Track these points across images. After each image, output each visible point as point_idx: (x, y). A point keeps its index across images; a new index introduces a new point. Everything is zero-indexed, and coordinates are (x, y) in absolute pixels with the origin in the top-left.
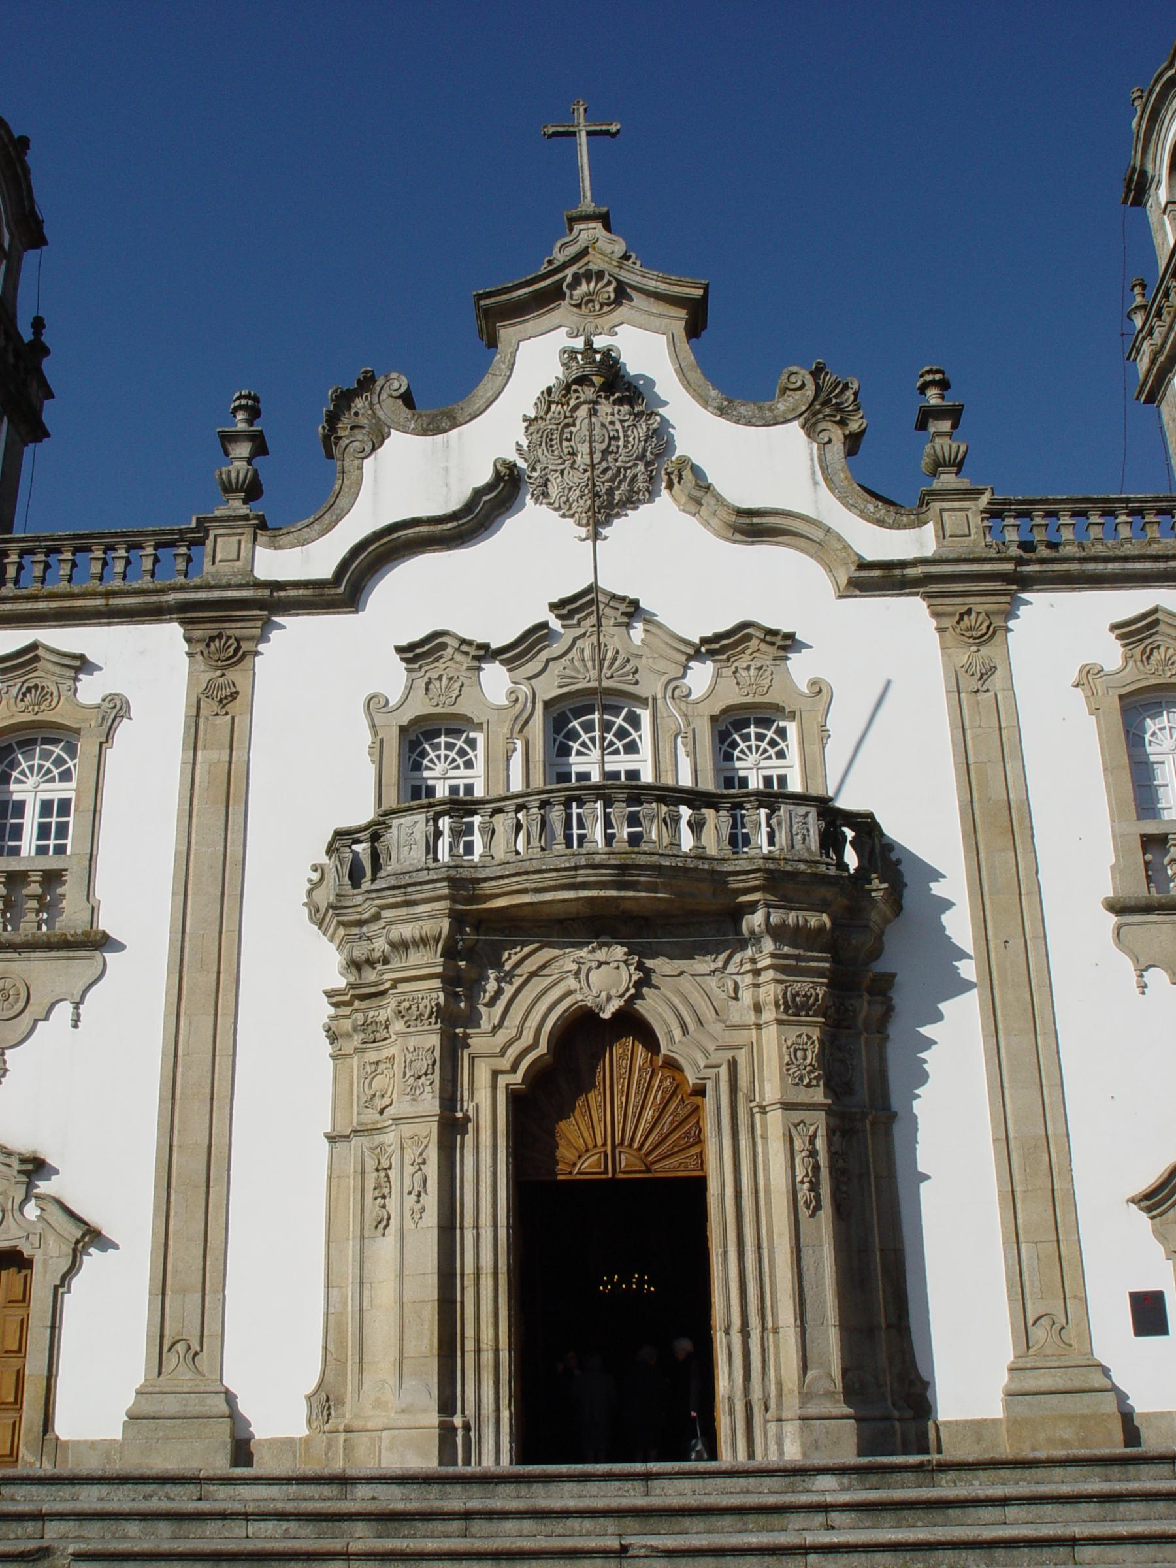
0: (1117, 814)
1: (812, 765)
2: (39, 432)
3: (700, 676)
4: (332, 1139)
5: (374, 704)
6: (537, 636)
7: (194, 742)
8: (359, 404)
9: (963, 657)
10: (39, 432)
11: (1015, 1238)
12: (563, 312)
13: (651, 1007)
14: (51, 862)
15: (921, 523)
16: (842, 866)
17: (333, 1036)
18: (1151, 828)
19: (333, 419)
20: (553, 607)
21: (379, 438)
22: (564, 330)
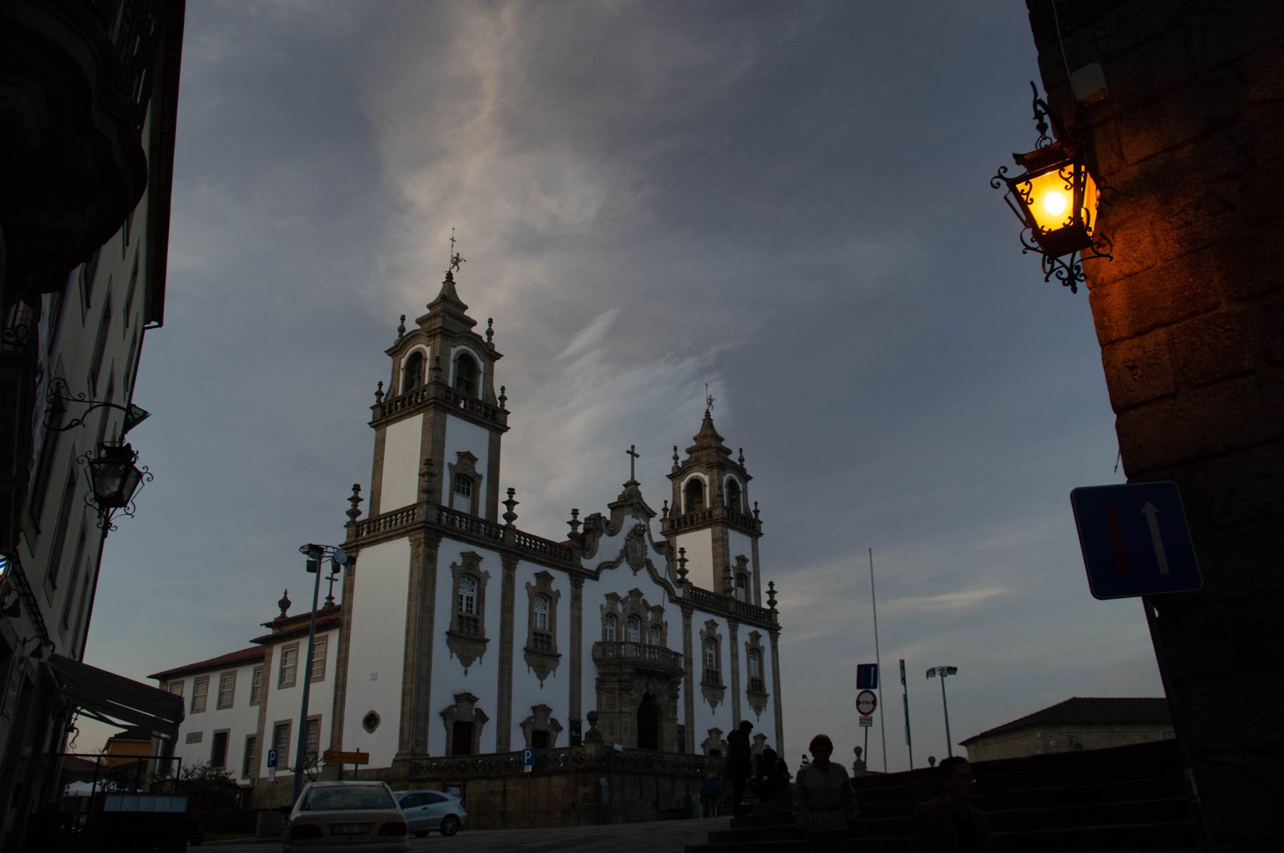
1: (663, 640)
5: (602, 606)
12: (631, 509)
15: (680, 588)
17: (598, 688)
20: (630, 592)
21: (602, 533)
22: (631, 515)
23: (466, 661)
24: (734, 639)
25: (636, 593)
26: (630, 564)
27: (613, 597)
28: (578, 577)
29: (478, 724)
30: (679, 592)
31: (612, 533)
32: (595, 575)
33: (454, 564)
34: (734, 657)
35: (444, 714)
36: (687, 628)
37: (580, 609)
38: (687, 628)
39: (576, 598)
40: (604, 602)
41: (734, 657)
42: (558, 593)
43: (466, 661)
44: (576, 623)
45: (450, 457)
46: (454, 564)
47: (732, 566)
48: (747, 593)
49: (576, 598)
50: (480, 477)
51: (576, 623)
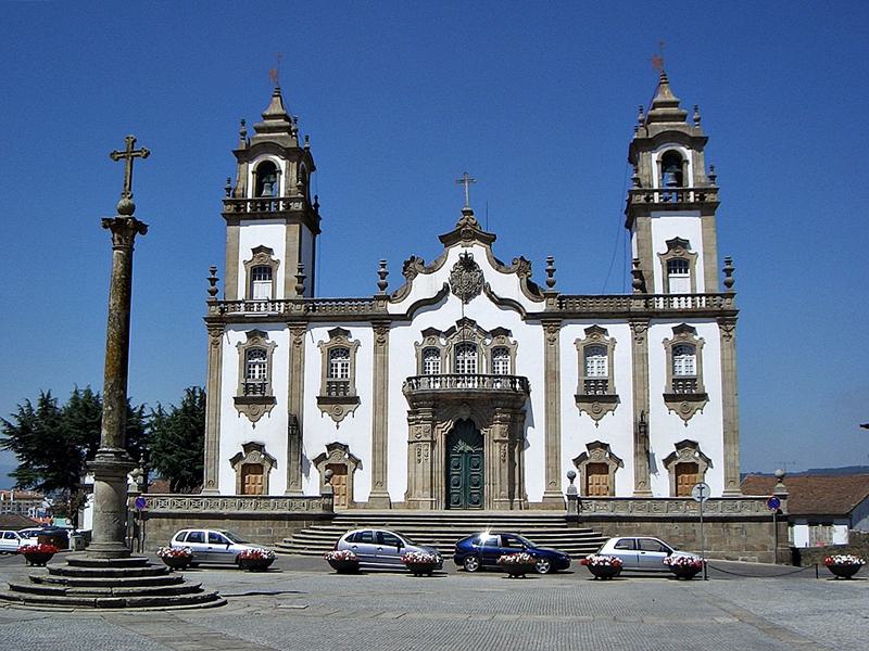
0: (580, 375)
1: (513, 363)
2: (319, 232)
3: (488, 341)
4: (409, 443)
5: (416, 344)
6: (452, 330)
7: (375, 352)
8: (411, 265)
9: (549, 336)
10: (319, 232)
11: (547, 467)
13: (474, 418)
14: (344, 379)
16: (515, 389)
18: (586, 378)
19: (405, 269)
23: (254, 418)
24: (639, 338)
25: (463, 322)
26: (458, 295)
27: (429, 333)
28: (382, 323)
29: (267, 465)
30: (539, 307)
31: (430, 270)
32: (406, 318)
33: (239, 343)
34: (640, 359)
35: (234, 461)
36: (552, 341)
37: (385, 352)
38: (552, 341)
39: (381, 343)
40: (420, 339)
41: (640, 359)
42: (358, 344)
43: (254, 418)
44: (382, 365)
45: (245, 254)
46: (239, 343)
47: (659, 255)
48: (693, 277)
49: (381, 343)
50: (278, 262)
51: (382, 365)
